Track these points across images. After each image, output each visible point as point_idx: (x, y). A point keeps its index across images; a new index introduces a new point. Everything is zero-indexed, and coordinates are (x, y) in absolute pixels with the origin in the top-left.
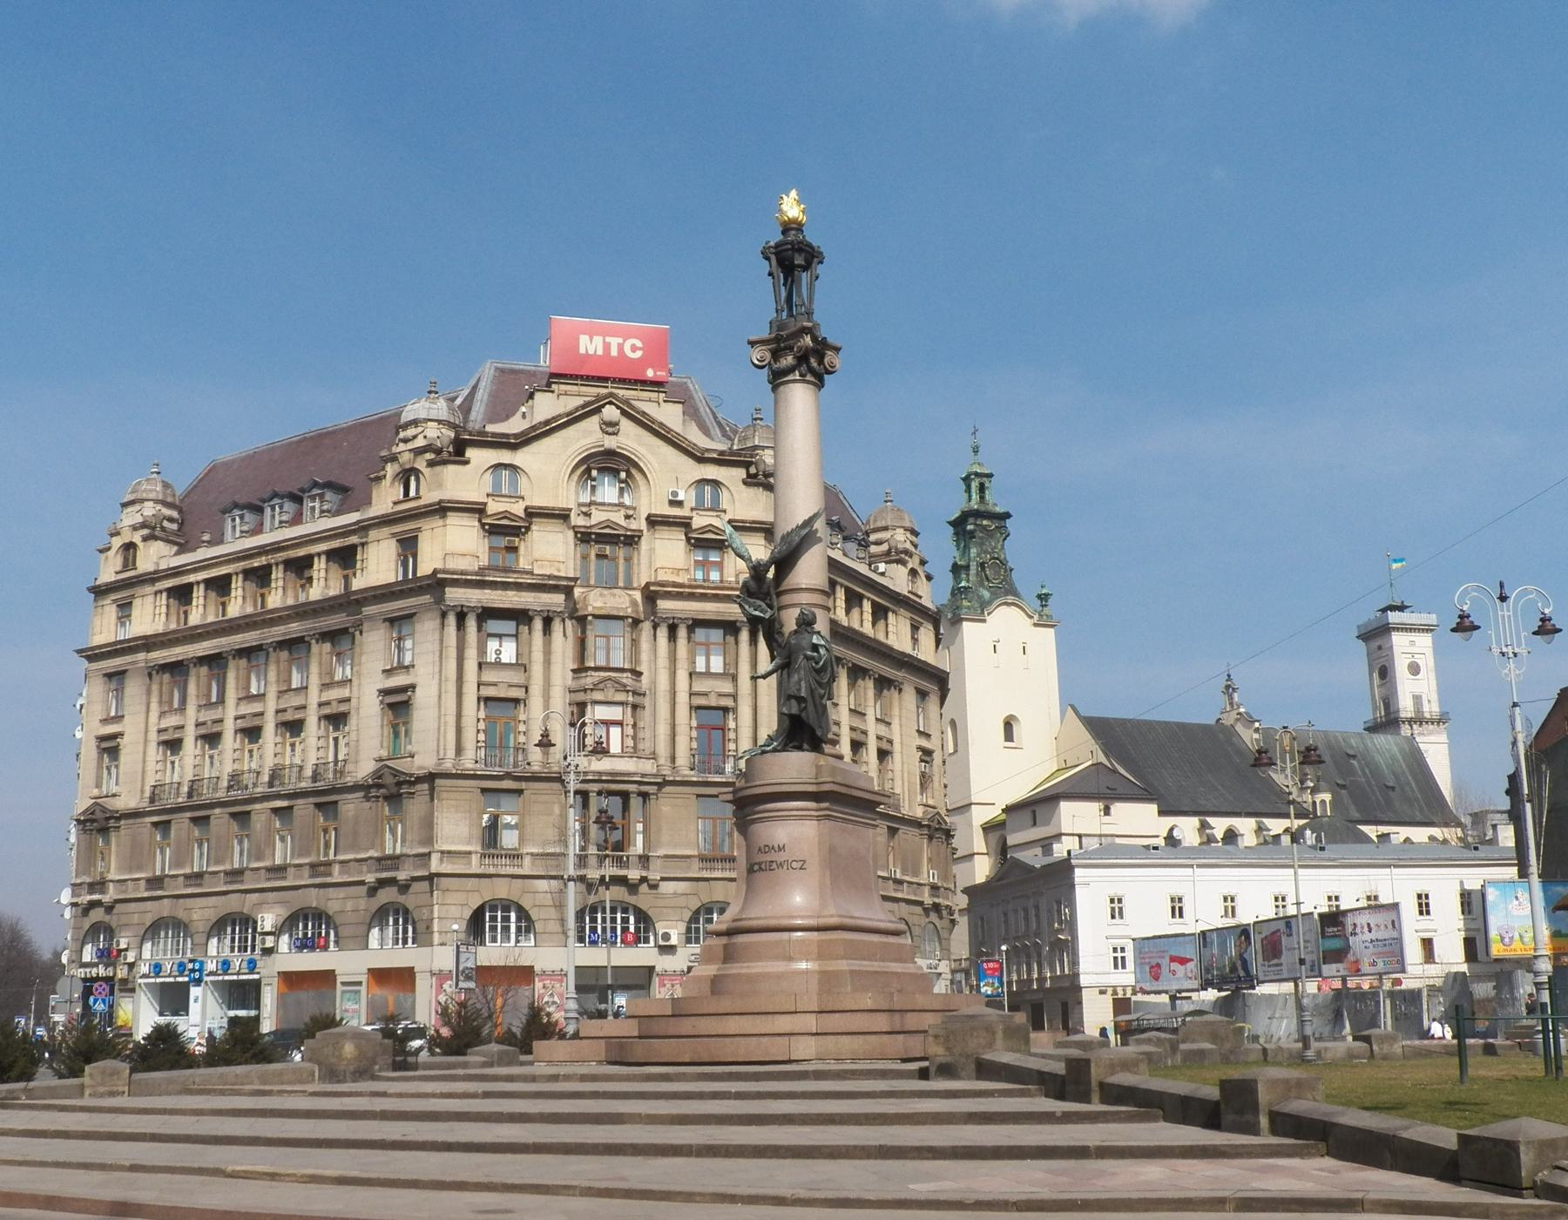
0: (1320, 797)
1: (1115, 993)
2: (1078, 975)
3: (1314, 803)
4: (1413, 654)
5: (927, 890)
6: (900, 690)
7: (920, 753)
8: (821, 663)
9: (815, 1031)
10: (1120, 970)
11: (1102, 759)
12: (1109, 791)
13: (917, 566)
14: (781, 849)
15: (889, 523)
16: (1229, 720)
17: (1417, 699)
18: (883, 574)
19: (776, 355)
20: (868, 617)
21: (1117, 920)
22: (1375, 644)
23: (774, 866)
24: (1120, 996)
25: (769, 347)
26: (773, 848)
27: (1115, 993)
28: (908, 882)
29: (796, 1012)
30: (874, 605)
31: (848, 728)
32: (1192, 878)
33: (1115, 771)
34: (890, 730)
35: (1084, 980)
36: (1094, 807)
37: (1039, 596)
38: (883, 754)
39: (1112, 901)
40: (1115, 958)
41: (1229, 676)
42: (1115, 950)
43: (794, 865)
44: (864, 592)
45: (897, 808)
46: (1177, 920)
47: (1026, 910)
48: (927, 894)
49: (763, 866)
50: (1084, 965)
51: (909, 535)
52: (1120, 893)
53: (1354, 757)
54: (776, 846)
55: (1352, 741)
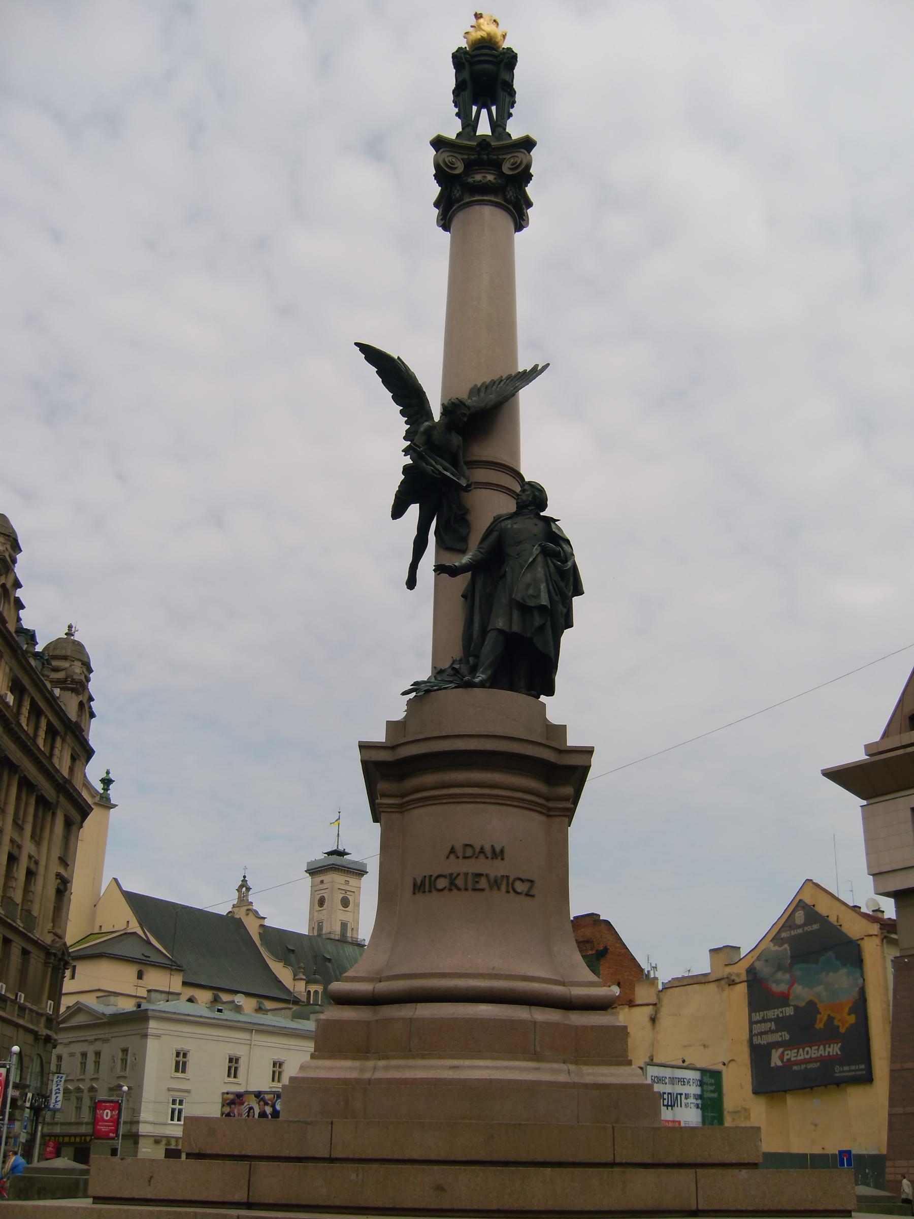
0: (313, 988)
1: (168, 1143)
2: (138, 1122)
3: (309, 992)
4: (346, 891)
5: (43, 1020)
6: (54, 814)
7: (60, 881)
8: (570, 564)
9: (694, 1207)
10: (175, 1122)
11: (135, 927)
12: (145, 958)
13: (85, 701)
14: (497, 854)
15: (69, 654)
16: (240, 914)
17: (344, 926)
18: (58, 698)
19: (470, 166)
20: (42, 734)
21: (179, 1075)
22: (318, 879)
23: (483, 883)
24: (173, 1147)
25: (466, 157)
26: (482, 851)
27: (168, 1143)
28: (31, 1010)
29: (612, 1165)
30: (49, 724)
31: (9, 838)
32: (249, 1042)
33: (149, 943)
34: (39, 851)
35: (143, 1129)
36: (130, 972)
37: (103, 781)
38: (30, 874)
39: (178, 1055)
40: (173, 1111)
41: (245, 877)
42: (174, 1102)
43: (519, 887)
44: (45, 710)
45: (31, 932)
46: (232, 1079)
47: (84, 1055)
48: (42, 1025)
49: (460, 882)
50: (144, 1116)
51: (85, 670)
52: (186, 1048)
53: (329, 960)
54: (488, 849)
55: (329, 947)
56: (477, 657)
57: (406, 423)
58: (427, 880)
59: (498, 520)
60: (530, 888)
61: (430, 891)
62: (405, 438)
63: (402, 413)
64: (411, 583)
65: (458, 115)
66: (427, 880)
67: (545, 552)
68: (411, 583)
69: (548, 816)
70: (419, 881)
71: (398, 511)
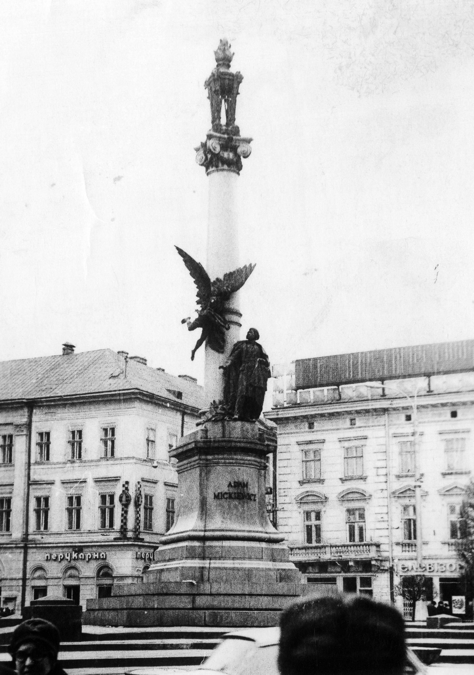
56: (234, 404)
57: (197, 288)
58: (220, 495)
59: (240, 343)
60: (255, 497)
61: (222, 498)
62: (197, 296)
63: (195, 282)
64: (193, 358)
65: (209, 98)
66: (220, 495)
67: (260, 362)
68: (193, 358)
69: (258, 469)
70: (216, 493)
71: (192, 328)
